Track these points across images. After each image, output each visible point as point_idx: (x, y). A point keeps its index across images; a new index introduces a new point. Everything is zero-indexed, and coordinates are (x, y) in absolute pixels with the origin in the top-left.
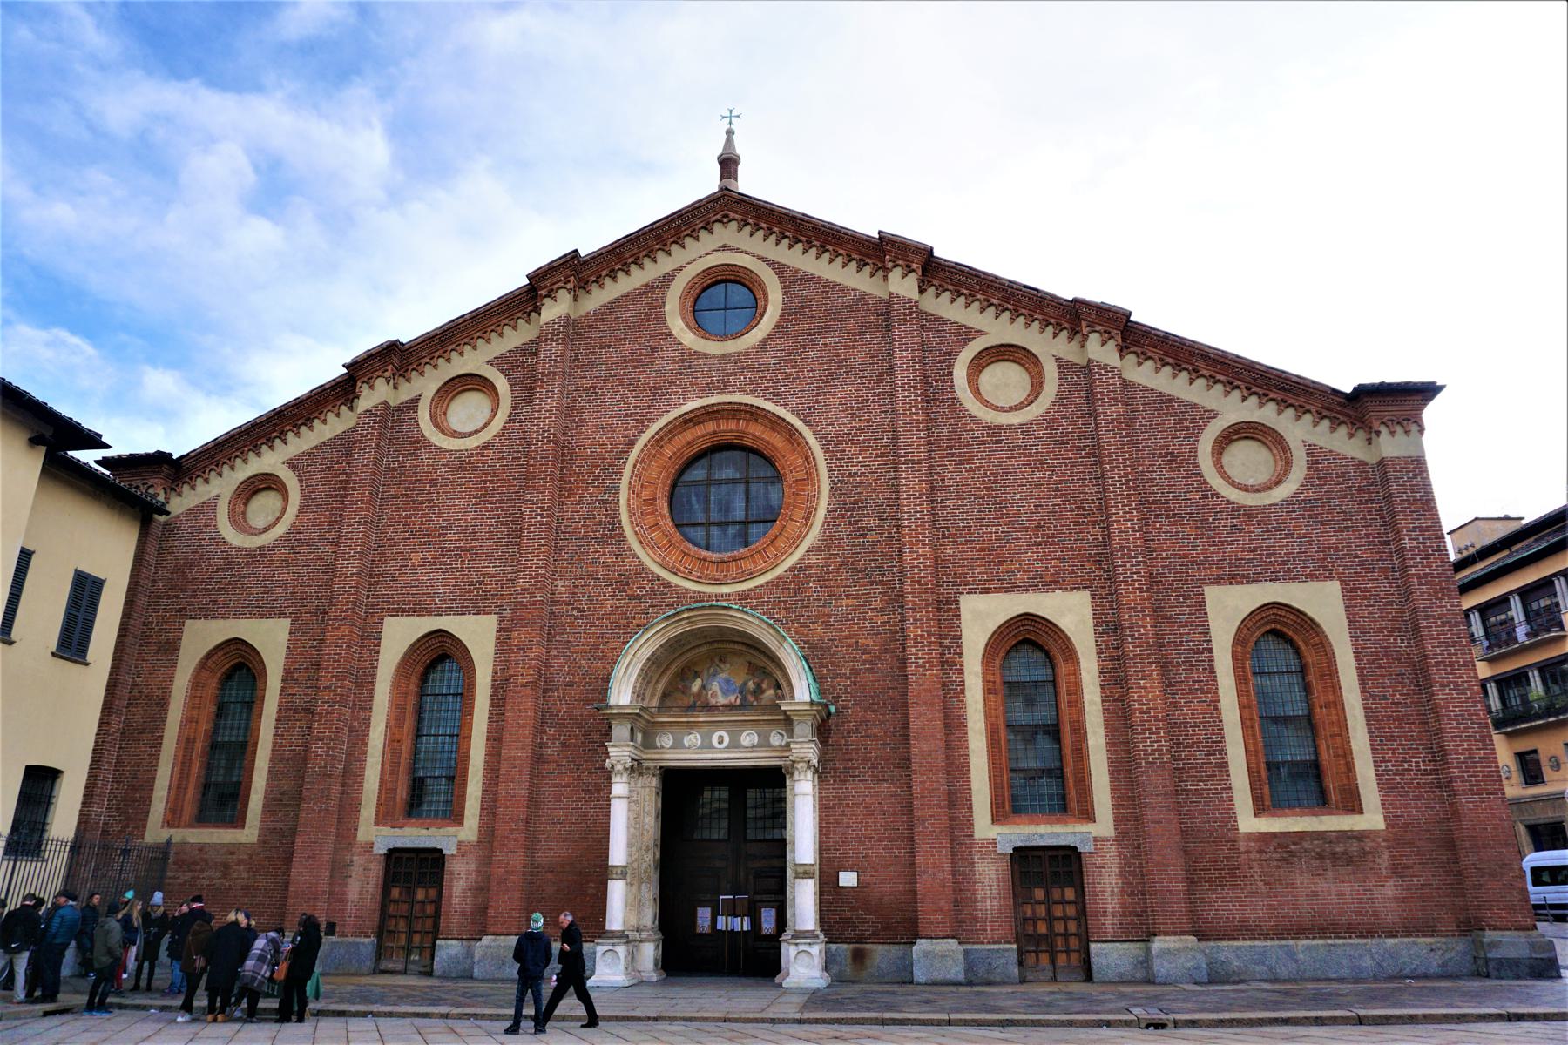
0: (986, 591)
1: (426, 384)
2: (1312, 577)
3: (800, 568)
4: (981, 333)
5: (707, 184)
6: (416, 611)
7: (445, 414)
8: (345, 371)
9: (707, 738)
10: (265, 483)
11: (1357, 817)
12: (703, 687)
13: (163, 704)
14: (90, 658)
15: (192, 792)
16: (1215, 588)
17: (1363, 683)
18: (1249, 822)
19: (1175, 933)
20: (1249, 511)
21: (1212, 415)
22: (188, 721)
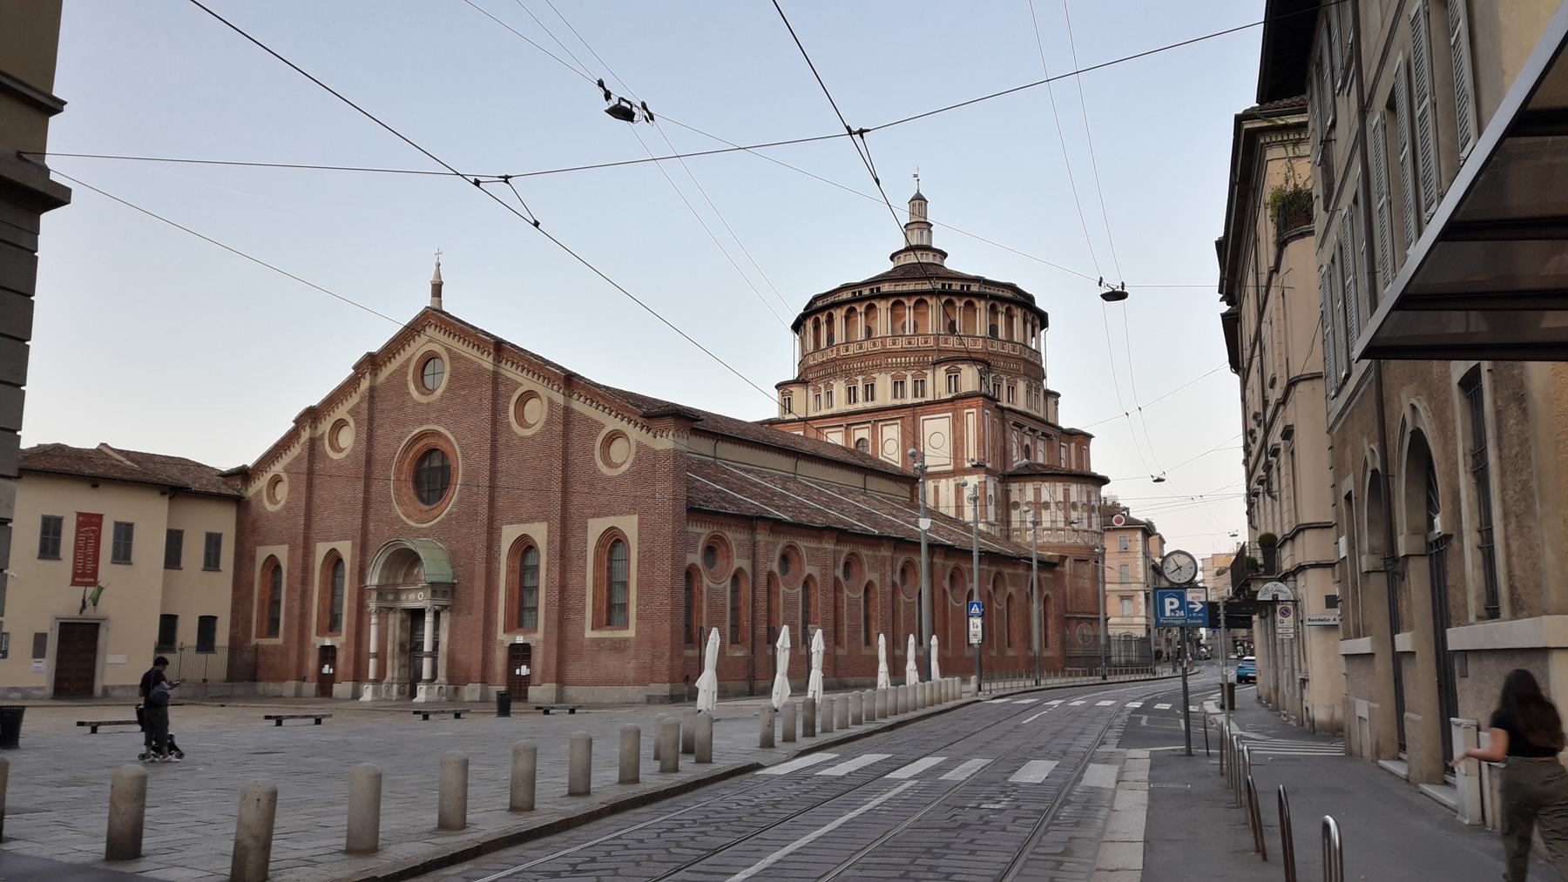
0: (512, 523)
1: (325, 426)
2: (628, 513)
3: (450, 514)
4: (521, 384)
5: (427, 301)
6: (327, 540)
7: (337, 439)
8: (293, 424)
9: (416, 595)
10: (276, 481)
11: (626, 631)
12: (418, 572)
13: (252, 584)
14: (221, 568)
15: (266, 623)
16: (592, 519)
17: (638, 567)
18: (589, 634)
19: (550, 682)
20: (610, 479)
21: (603, 426)
22: (262, 592)
